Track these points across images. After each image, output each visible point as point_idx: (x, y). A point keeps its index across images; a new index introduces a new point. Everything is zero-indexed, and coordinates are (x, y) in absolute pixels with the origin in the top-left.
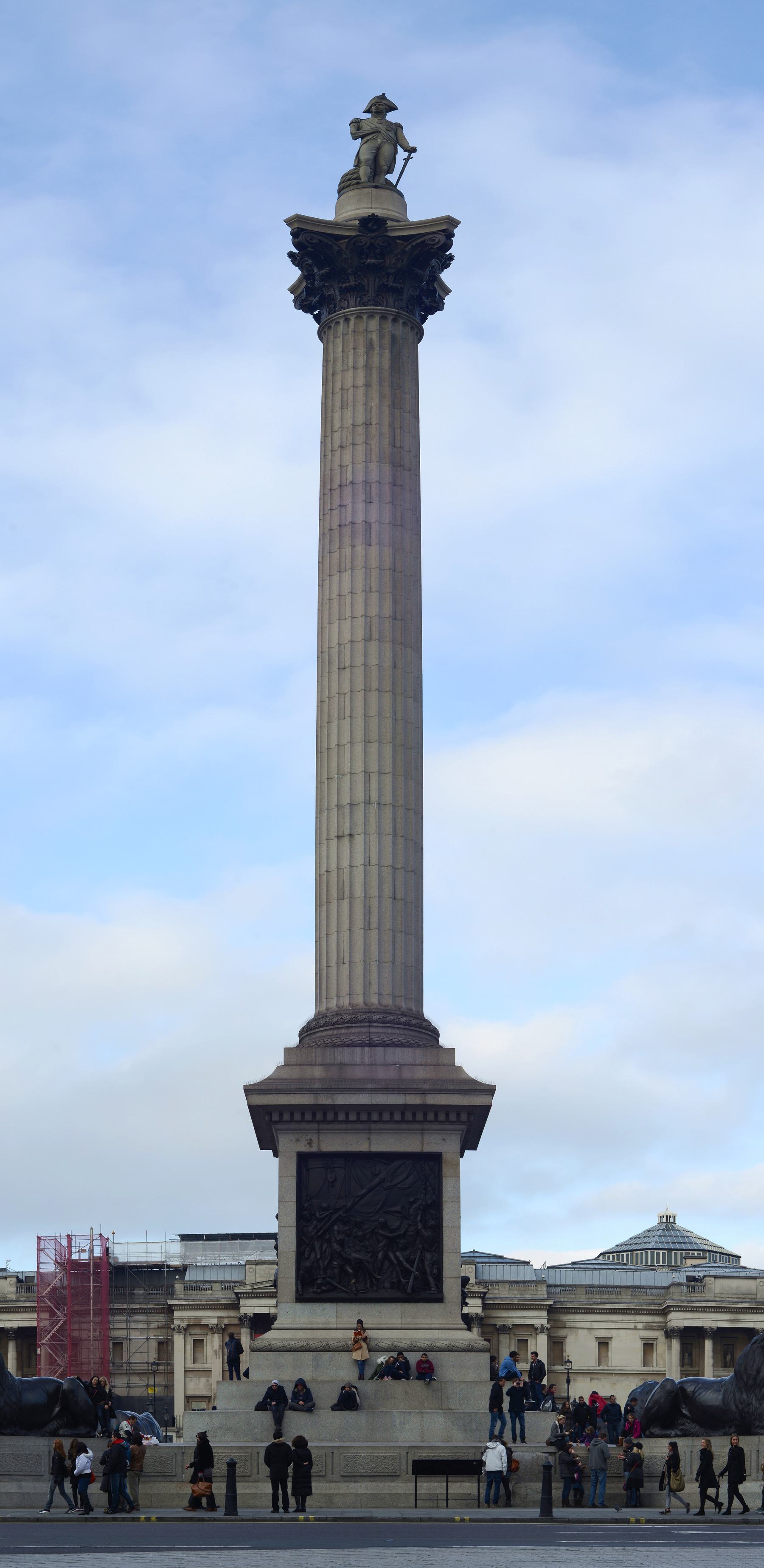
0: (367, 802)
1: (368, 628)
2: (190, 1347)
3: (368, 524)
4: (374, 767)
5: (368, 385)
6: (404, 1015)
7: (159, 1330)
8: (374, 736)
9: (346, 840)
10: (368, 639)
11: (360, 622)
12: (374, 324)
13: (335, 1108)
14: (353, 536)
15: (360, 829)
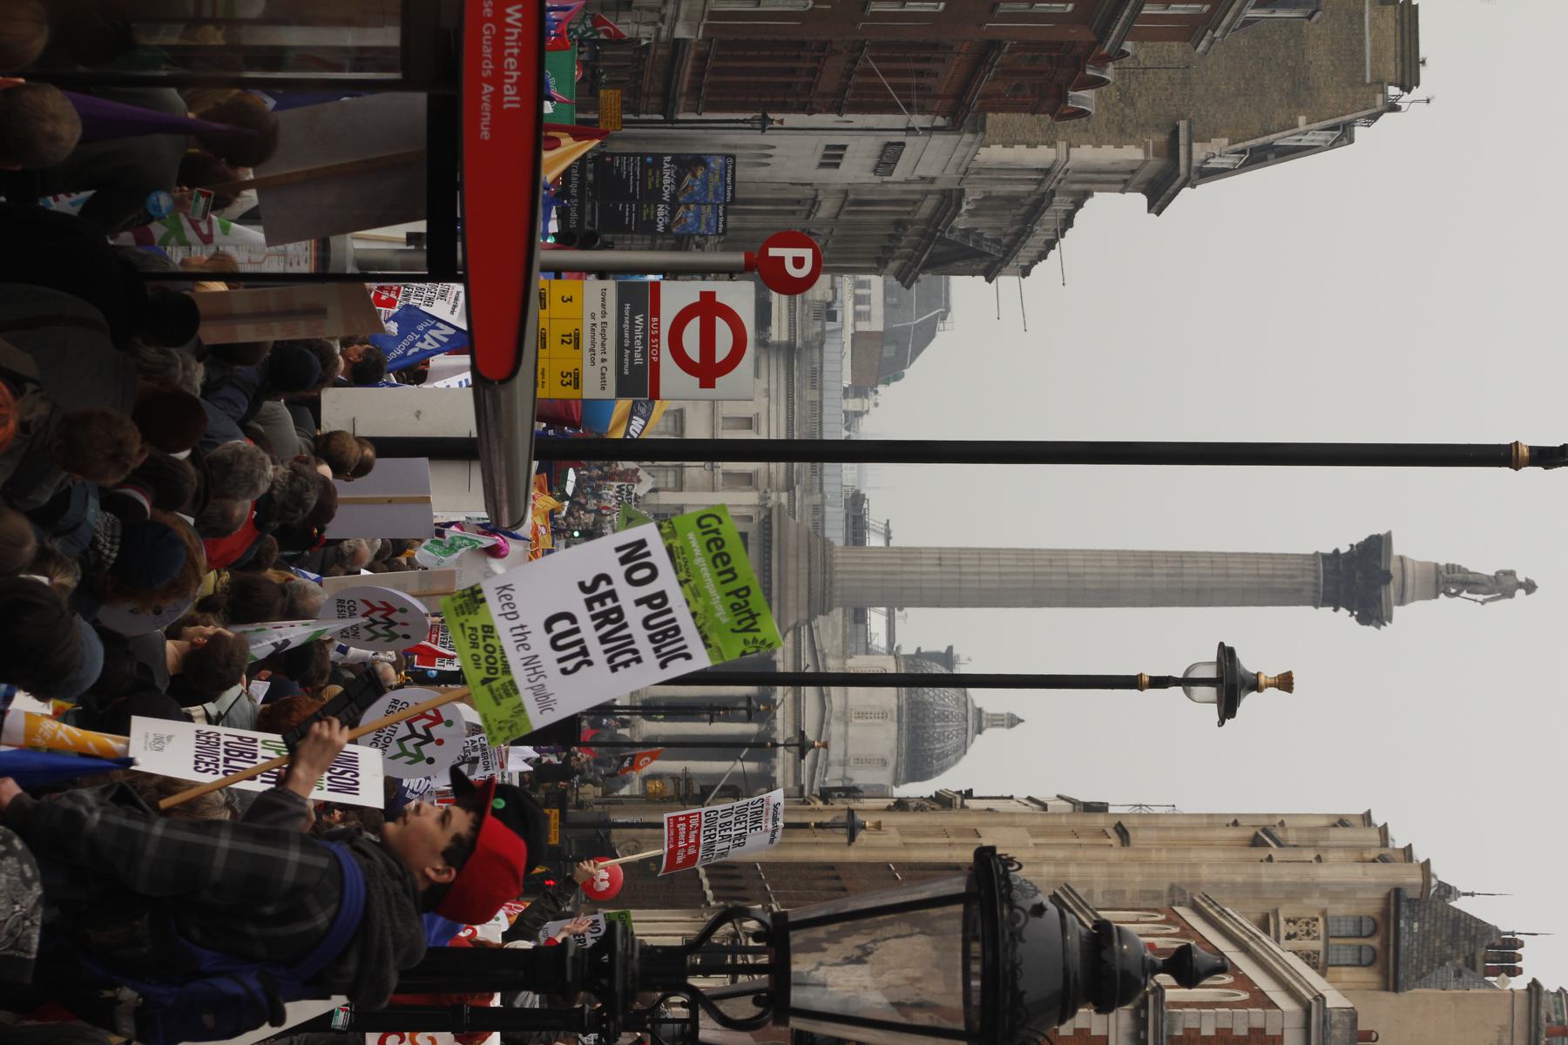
0: (961, 573)
1: (1078, 575)
2: (744, 511)
3: (1152, 575)
4: (983, 577)
5: (1259, 576)
6: (830, 592)
7: (766, 475)
8: (1003, 578)
9: (938, 562)
10: (1068, 574)
11: (1081, 570)
12: (1311, 579)
13: (770, 553)
14: (1143, 567)
15: (944, 569)
